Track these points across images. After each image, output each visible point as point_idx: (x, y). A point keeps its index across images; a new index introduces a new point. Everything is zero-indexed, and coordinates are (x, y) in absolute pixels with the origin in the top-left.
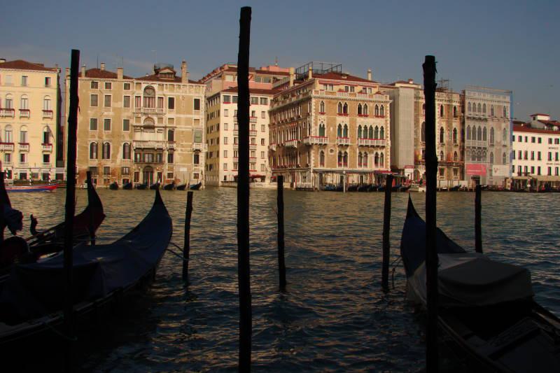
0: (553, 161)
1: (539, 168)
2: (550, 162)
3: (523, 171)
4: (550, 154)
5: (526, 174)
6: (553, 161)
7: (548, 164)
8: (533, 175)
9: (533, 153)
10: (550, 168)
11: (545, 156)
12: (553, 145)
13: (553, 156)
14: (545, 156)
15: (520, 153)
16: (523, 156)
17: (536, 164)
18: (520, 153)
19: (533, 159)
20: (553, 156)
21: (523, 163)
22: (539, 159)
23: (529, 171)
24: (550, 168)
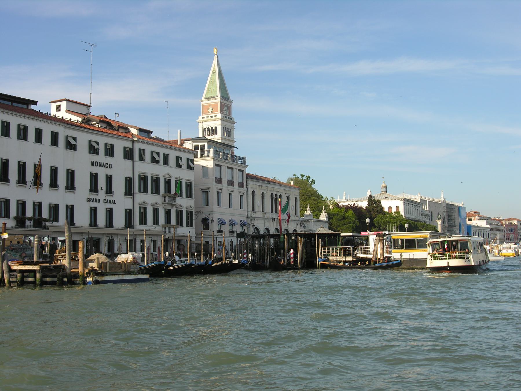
0: (101, 195)
1: (70, 210)
2: (93, 196)
3: (29, 213)
4: (94, 177)
5: (38, 222)
6: (101, 195)
7: (89, 200)
8: (55, 224)
9: (54, 171)
10: (94, 212)
11: (82, 182)
12: (101, 158)
13: (102, 183)
14: (82, 182)
15: (22, 167)
16: (30, 176)
17: (61, 197)
18: (22, 167)
19: (54, 184)
20: (102, 183)
21: (29, 195)
22: (71, 186)
23: (45, 214)
24: (94, 212)
